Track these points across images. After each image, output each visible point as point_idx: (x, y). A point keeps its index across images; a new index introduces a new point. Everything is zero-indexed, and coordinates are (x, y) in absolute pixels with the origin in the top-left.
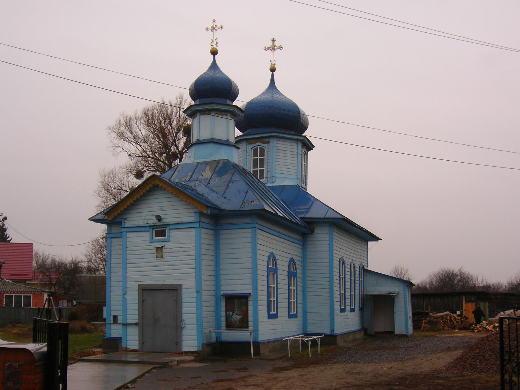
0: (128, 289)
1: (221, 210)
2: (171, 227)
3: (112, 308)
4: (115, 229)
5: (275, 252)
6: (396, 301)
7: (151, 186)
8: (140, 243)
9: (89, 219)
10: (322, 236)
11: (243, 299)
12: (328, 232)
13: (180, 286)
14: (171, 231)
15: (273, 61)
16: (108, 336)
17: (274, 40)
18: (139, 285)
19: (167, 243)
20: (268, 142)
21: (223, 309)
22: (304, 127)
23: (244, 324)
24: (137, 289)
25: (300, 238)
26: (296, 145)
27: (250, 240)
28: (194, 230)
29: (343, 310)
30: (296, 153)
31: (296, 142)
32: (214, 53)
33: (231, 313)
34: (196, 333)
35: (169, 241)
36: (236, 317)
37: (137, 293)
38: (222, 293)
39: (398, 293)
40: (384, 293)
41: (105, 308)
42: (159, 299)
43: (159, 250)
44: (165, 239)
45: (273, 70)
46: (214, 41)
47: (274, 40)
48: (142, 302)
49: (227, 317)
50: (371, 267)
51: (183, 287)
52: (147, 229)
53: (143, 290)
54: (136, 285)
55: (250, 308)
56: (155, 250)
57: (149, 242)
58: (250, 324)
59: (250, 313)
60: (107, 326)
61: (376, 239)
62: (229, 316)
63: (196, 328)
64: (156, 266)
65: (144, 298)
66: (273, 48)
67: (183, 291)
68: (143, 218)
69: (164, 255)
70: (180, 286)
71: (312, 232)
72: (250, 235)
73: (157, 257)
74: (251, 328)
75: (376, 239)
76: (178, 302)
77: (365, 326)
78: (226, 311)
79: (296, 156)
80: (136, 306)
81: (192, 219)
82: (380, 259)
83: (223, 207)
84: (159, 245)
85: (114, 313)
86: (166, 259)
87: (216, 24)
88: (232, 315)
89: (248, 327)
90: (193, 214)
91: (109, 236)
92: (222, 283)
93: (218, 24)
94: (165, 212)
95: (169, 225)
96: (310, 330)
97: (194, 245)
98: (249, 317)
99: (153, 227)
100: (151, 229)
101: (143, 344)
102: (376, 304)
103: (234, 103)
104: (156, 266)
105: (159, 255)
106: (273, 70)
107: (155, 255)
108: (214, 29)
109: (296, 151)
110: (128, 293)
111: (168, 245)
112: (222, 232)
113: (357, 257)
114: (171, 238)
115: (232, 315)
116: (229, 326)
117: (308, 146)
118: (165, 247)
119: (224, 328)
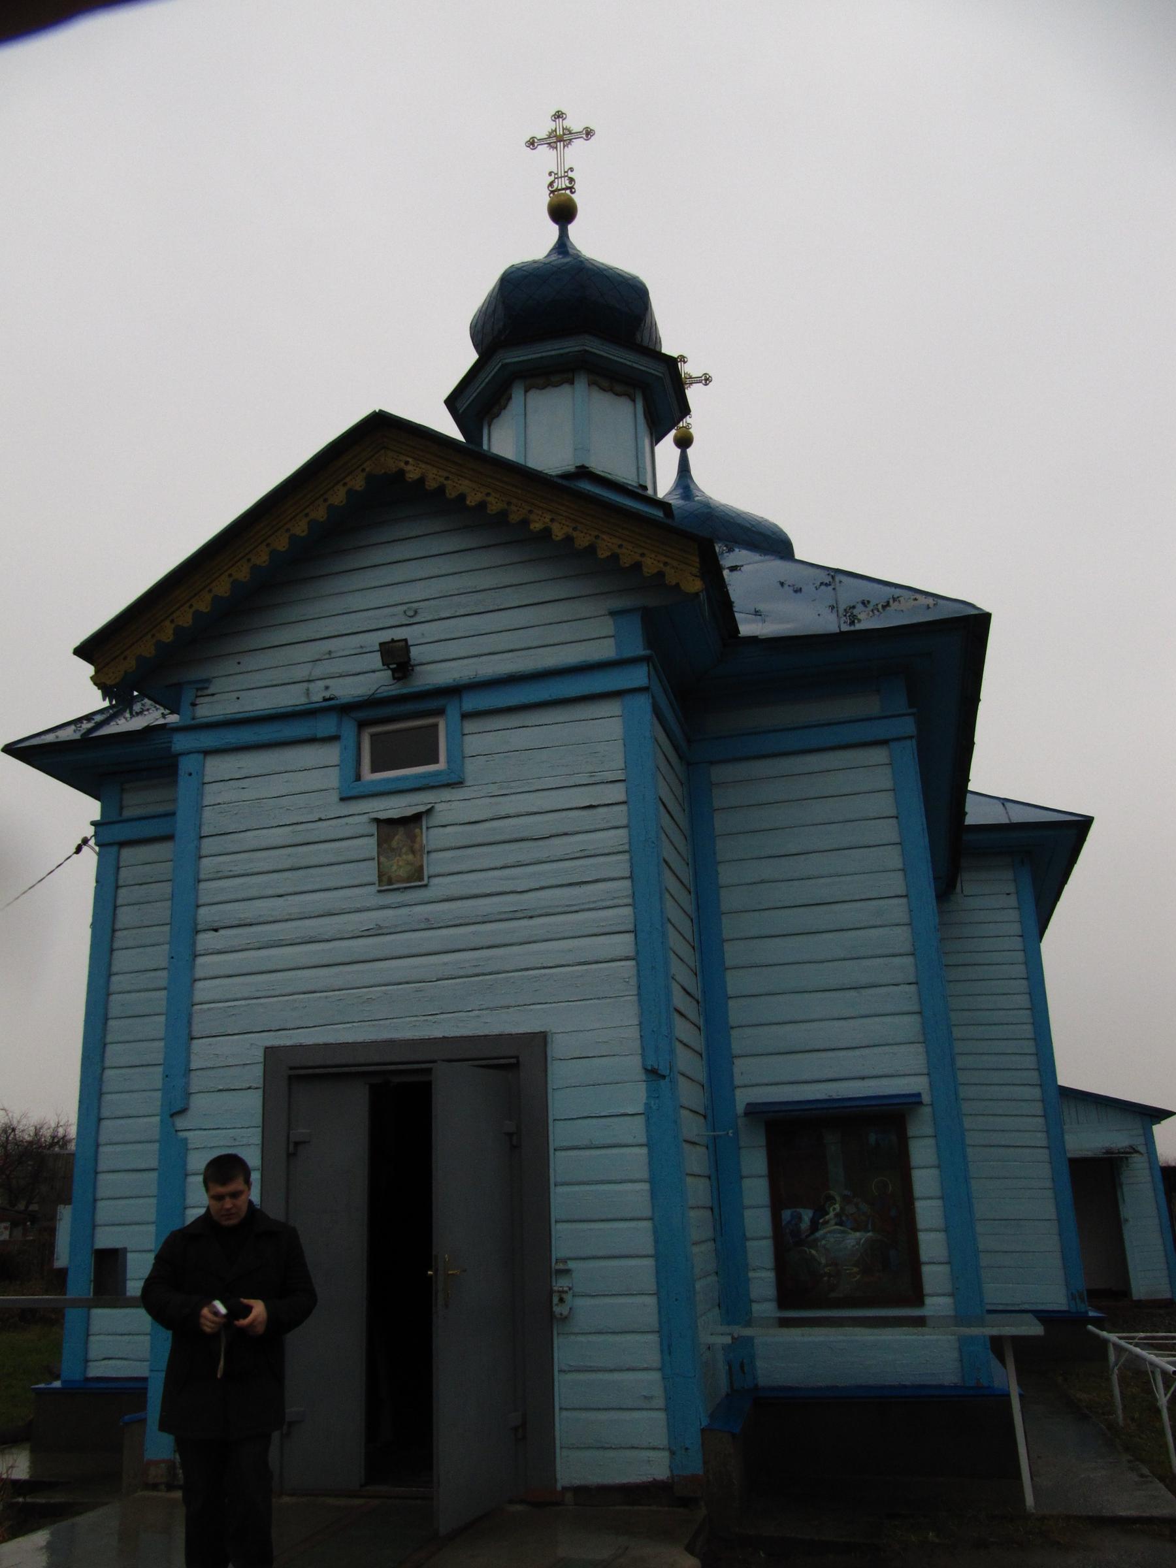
0: (197, 1082)
2: (471, 702)
3: (105, 1211)
4: (138, 802)
8: (277, 809)
12: (1011, 888)
13: (540, 1040)
14: (470, 726)
16: (69, 1369)
18: (270, 1051)
19: (446, 794)
21: (756, 1190)
23: (891, 1280)
24: (256, 1074)
28: (613, 708)
32: (563, 212)
33: (807, 1215)
34: (653, 1357)
35: (459, 784)
36: (842, 1241)
37: (253, 1102)
38: (743, 1098)
40: (1090, 1154)
41: (65, 1214)
43: (399, 831)
44: (437, 774)
49: (786, 1243)
51: (559, 1047)
52: (327, 725)
53: (290, 1078)
54: (252, 1049)
55: (925, 1181)
56: (373, 842)
57: (335, 797)
60: (72, 1316)
63: (653, 1321)
64: (377, 932)
65: (786, 586)
67: (560, 1073)
68: (301, 672)
69: (434, 864)
70: (540, 1040)
73: (386, 881)
74: (937, 1304)
78: (777, 1204)
81: (606, 650)
85: (106, 1239)
86: (440, 887)
87: (566, 123)
88: (815, 1226)
89: (918, 1298)
90: (607, 626)
91: (110, 838)
92: (739, 1041)
93: (574, 123)
96: (995, 1293)
97: (617, 793)
99: (361, 712)
100: (348, 730)
104: (377, 932)
105: (398, 866)
107: (369, 872)
108: (559, 139)
110: (199, 1103)
111: (450, 807)
112: (719, 773)
114: (471, 768)
115: (815, 1226)
116: (803, 1290)
118: (436, 819)
119: (766, 1308)
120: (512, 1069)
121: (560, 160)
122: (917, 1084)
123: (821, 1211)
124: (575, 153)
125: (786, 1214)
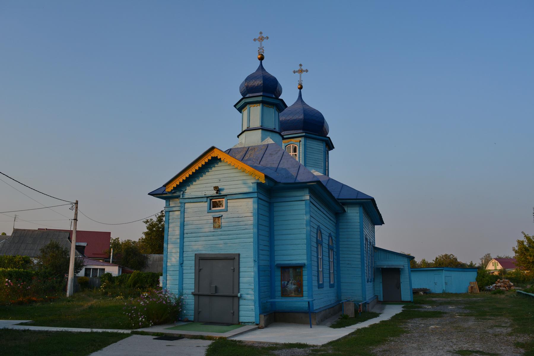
0: (185, 259)
1: (276, 182)
2: (229, 197)
5: (321, 226)
7: (210, 158)
8: (197, 214)
9: (149, 194)
11: (298, 268)
17: (301, 65)
29: (368, 282)
32: (261, 59)
33: (286, 282)
36: (292, 287)
37: (193, 262)
38: (277, 262)
42: (216, 268)
45: (301, 88)
46: (261, 48)
47: (301, 65)
48: (198, 271)
52: (205, 199)
55: (305, 278)
58: (305, 293)
59: (305, 283)
62: (284, 285)
66: (301, 71)
73: (214, 227)
76: (236, 272)
77: (376, 294)
80: (193, 276)
83: (278, 180)
84: (217, 215)
86: (223, 229)
88: (287, 284)
93: (264, 35)
94: (223, 184)
95: (226, 195)
98: (304, 287)
99: (211, 198)
101: (199, 314)
103: (280, 98)
105: (217, 225)
108: (261, 39)
110: (185, 262)
115: (287, 284)
117: (330, 146)
120: (233, 259)
121: (261, 44)
122: (305, 262)
123: (288, 282)
124: (265, 43)
125: (283, 282)
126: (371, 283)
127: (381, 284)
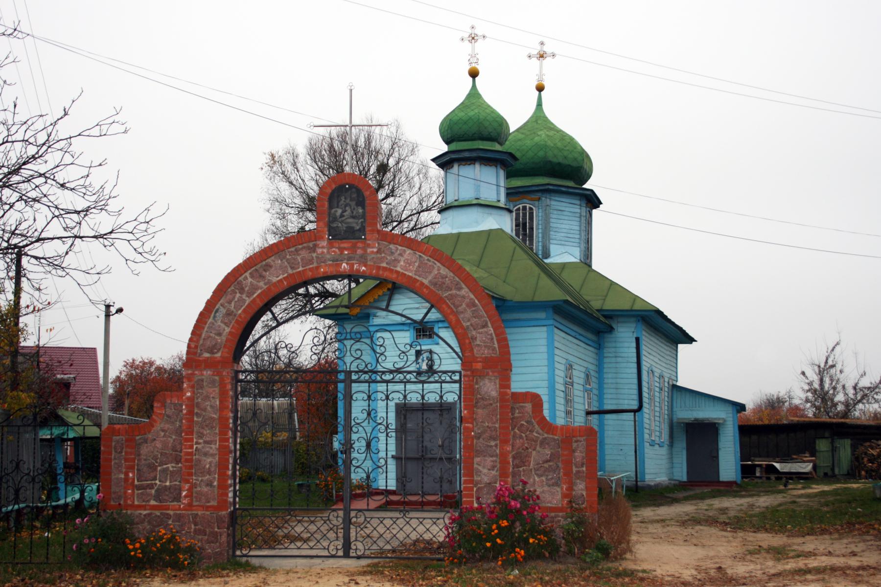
6: (721, 432)
10: (625, 336)
15: (541, 75)
17: (542, 44)
20: (539, 199)
22: (587, 176)
25: (594, 338)
26: (578, 202)
27: (544, 342)
30: (578, 215)
31: (578, 198)
32: (474, 74)
39: (725, 421)
45: (540, 89)
47: (542, 44)
50: (681, 383)
61: (690, 340)
66: (542, 56)
71: (611, 329)
72: (545, 335)
75: (690, 340)
79: (578, 219)
82: (694, 369)
83: (508, 297)
93: (479, 31)
102: (698, 436)
106: (540, 89)
108: (473, 38)
109: (579, 211)
113: (664, 365)
117: (593, 201)
121: (473, 49)
126: (664, 451)
127: (685, 452)
